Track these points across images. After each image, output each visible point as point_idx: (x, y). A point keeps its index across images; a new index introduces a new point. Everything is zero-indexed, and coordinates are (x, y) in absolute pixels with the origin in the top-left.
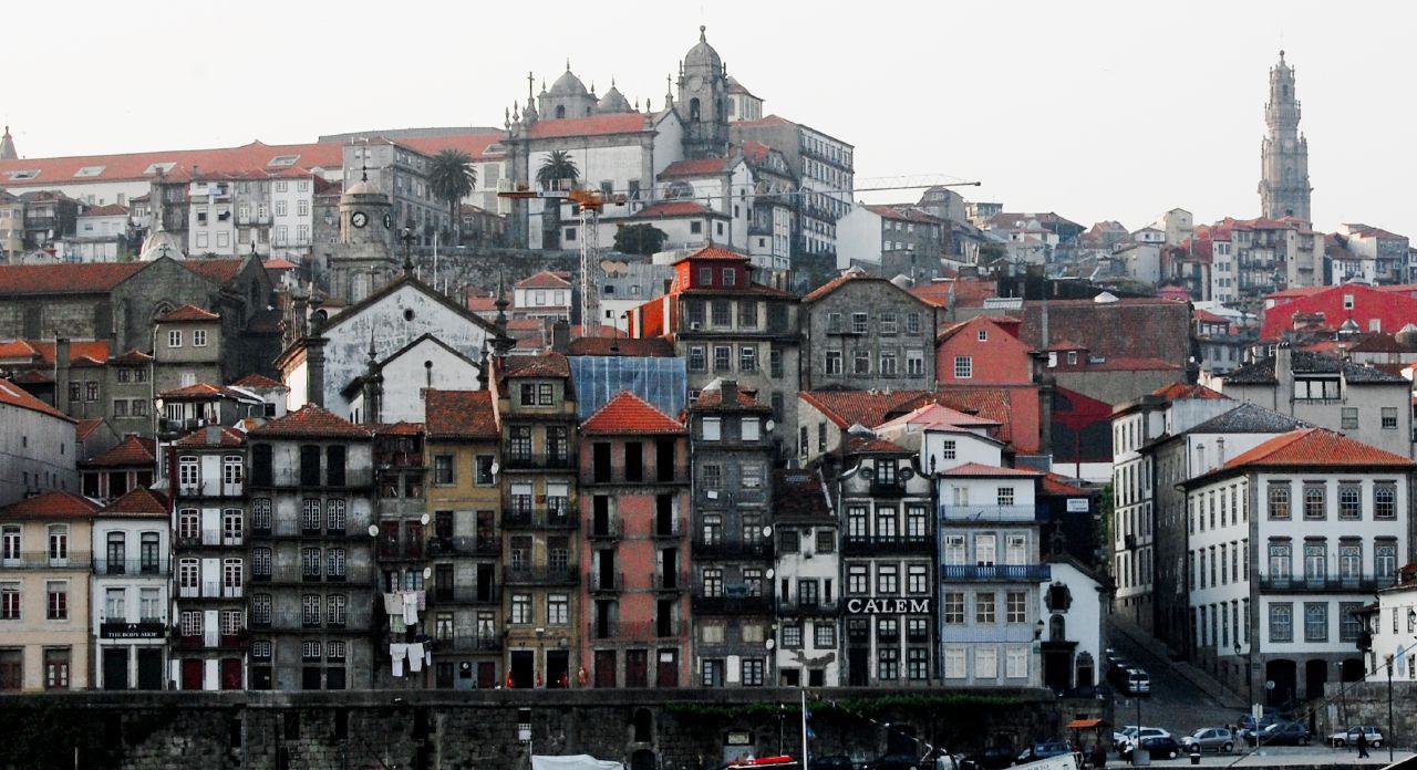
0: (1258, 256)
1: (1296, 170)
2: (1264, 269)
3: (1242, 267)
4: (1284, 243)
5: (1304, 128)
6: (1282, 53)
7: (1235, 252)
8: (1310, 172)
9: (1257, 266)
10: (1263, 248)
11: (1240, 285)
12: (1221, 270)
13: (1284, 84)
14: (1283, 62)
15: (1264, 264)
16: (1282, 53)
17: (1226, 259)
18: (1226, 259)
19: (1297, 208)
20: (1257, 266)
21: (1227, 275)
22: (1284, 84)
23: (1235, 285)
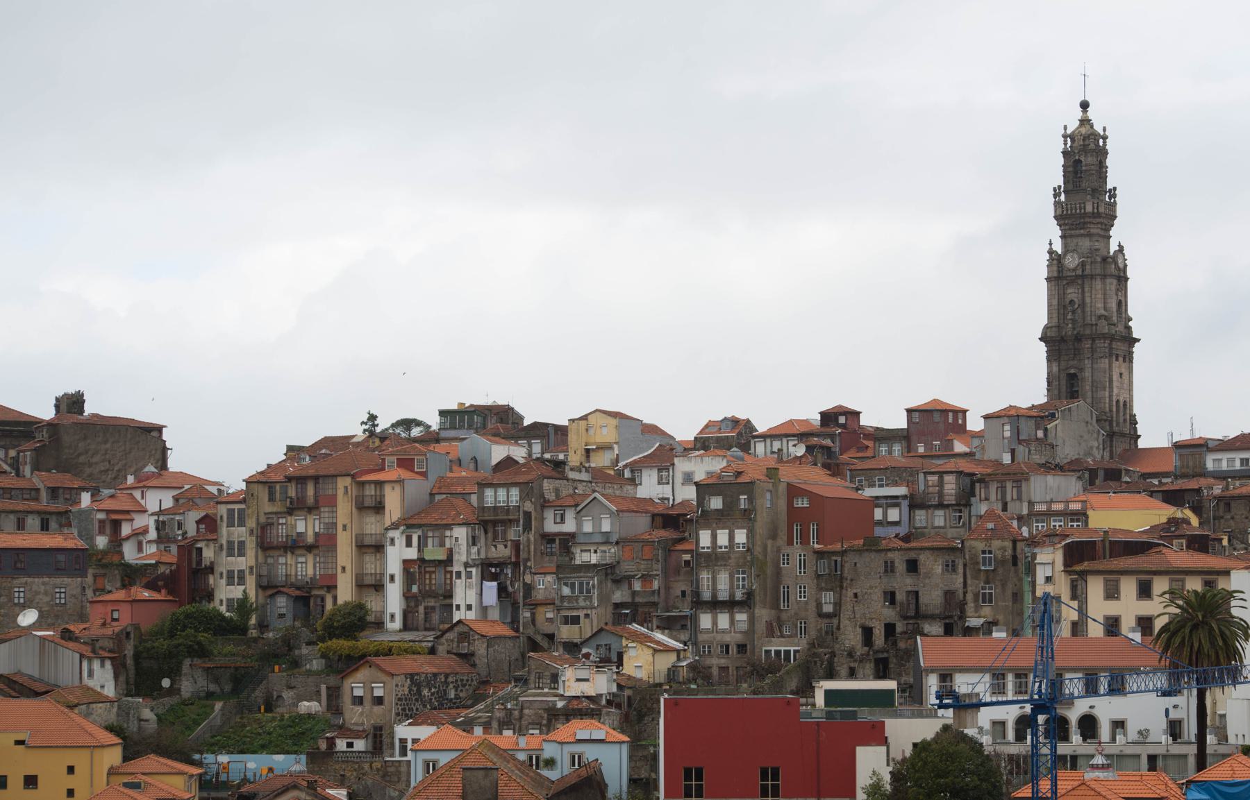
0: (301, 527)
1: (1083, 305)
2: (310, 548)
3: (265, 546)
4: (332, 502)
5: (1118, 235)
6: (1085, 105)
7: (251, 523)
8: (1134, 308)
9: (295, 546)
10: (310, 510)
11: (259, 576)
12: (230, 554)
13: (1085, 159)
14: (1085, 122)
15: (310, 539)
16: (1085, 105)
17: (239, 533)
18: (239, 533)
19: (1081, 370)
20: (295, 546)
21: (241, 563)
22: (1085, 159)
23: (251, 582)
